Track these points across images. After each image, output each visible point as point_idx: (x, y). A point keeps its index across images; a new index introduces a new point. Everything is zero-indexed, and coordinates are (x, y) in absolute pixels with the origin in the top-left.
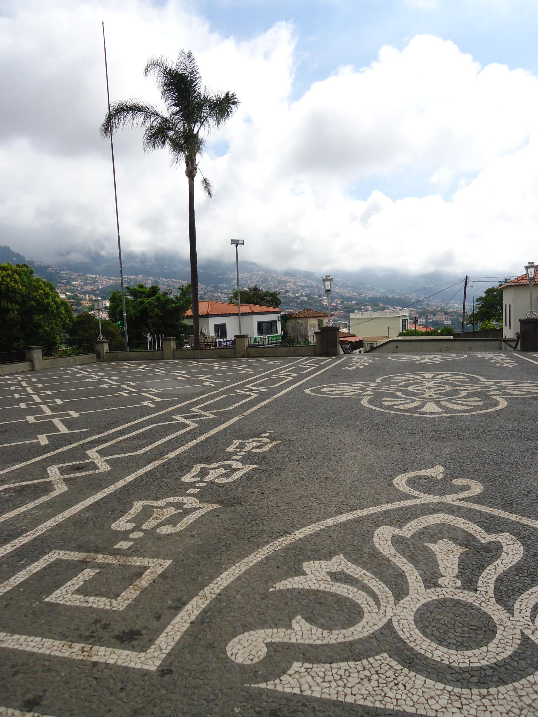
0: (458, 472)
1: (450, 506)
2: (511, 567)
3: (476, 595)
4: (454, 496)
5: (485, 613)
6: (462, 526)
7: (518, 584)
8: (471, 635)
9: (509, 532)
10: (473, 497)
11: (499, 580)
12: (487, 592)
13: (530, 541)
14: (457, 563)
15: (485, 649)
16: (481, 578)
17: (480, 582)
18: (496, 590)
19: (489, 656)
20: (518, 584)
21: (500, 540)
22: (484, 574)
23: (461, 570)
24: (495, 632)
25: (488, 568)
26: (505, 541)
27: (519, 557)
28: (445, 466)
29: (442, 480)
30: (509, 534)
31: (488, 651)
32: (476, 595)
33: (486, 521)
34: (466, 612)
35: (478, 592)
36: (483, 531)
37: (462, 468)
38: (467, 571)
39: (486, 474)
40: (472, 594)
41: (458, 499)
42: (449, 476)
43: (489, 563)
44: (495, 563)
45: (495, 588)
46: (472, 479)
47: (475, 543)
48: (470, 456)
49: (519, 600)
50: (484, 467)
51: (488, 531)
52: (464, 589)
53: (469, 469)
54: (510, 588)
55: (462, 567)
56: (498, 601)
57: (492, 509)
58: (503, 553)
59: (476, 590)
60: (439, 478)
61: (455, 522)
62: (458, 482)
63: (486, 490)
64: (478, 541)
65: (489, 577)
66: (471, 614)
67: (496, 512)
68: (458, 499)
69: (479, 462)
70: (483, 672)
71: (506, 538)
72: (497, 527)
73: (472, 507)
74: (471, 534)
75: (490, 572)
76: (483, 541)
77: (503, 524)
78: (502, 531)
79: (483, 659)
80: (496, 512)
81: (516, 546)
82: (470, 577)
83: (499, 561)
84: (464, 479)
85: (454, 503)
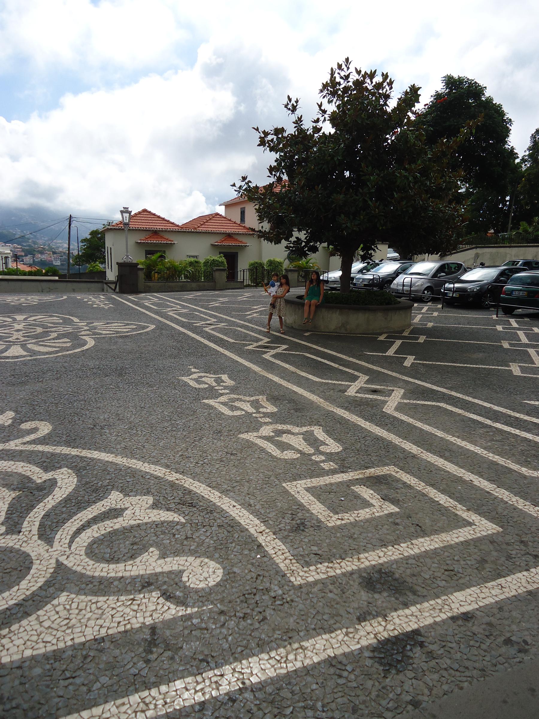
0: (28, 416)
1: (12, 452)
2: (61, 501)
3: (19, 537)
4: (19, 441)
5: (24, 552)
6: (20, 470)
7: (64, 516)
8: (4, 579)
9: (67, 467)
10: (38, 438)
11: (47, 516)
12: (30, 531)
13: (85, 471)
14: (6, 509)
15: (17, 587)
16: (27, 519)
17: (26, 523)
18: (42, 526)
19: (18, 595)
20: (64, 516)
21: (56, 476)
22: (31, 514)
23: (8, 515)
24: (29, 568)
25: (38, 507)
26: (61, 476)
27: (70, 489)
28: (16, 411)
29: (9, 426)
30: (66, 469)
31: (18, 590)
32: (19, 537)
33: (47, 460)
34: (4, 557)
35: (21, 534)
36: (42, 471)
37: (34, 411)
38: (14, 515)
39: (58, 414)
40: (14, 537)
41: (22, 444)
42: (17, 422)
43: (39, 501)
44: (46, 501)
45: (40, 525)
46: (42, 420)
47: (30, 485)
48: (46, 398)
49: (61, 530)
50: (57, 407)
51: (46, 470)
52: (7, 534)
53: (41, 411)
54: (55, 521)
55: (9, 512)
56: (41, 536)
57: (55, 447)
58: (57, 489)
59: (20, 532)
60: (6, 424)
61: (14, 467)
62: (26, 426)
63: (54, 430)
64: (34, 482)
65: (36, 516)
66: (9, 558)
67: (58, 450)
68: (22, 444)
69: (53, 403)
70: (8, 613)
71: (62, 474)
72: (56, 464)
73: (36, 449)
74: (28, 477)
75: (38, 510)
76: (39, 481)
77: (63, 461)
78: (60, 468)
79: (12, 599)
80: (58, 450)
81: (71, 479)
82: (17, 520)
83: (50, 497)
84: (33, 422)
85: (17, 448)
